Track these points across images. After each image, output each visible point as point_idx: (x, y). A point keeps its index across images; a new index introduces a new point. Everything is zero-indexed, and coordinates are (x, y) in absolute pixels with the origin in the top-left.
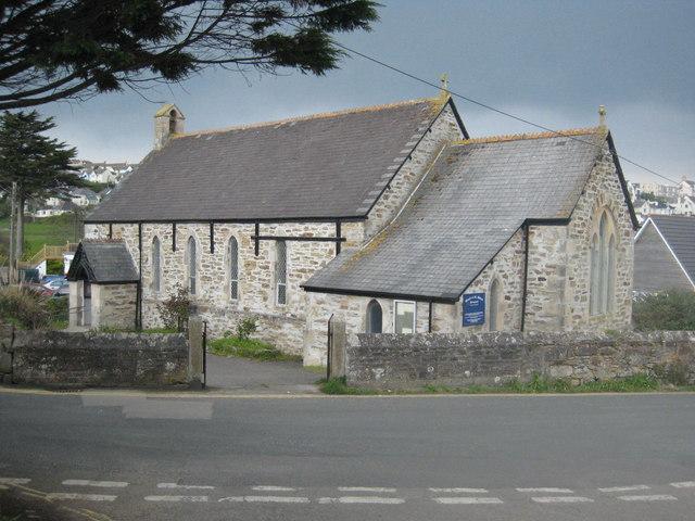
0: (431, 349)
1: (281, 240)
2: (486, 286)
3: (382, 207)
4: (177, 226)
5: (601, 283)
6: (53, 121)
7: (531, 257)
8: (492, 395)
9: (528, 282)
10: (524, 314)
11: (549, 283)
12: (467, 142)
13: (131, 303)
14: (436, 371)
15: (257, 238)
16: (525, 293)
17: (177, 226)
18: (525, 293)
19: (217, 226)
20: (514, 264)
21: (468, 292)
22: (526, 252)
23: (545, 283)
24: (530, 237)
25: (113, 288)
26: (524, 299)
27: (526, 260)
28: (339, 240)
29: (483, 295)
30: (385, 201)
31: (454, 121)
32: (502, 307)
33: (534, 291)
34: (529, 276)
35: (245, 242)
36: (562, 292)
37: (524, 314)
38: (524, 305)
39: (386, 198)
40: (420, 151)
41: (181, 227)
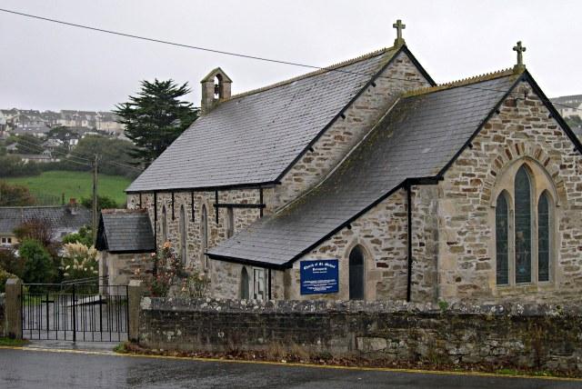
0: (220, 314)
1: (230, 207)
2: (342, 254)
3: (303, 171)
4: (175, 194)
5: (524, 246)
6: (186, 88)
7: (414, 220)
8: (272, 363)
9: (413, 248)
10: (409, 283)
11: (427, 249)
12: (434, 89)
13: (148, 272)
14: (226, 335)
15: (217, 206)
16: (410, 260)
17: (175, 194)
18: (410, 260)
19: (197, 195)
20: (392, 228)
21: (308, 258)
22: (410, 214)
23: (424, 248)
24: (412, 198)
25: (127, 257)
26: (410, 267)
27: (410, 223)
28: (262, 206)
29: (335, 262)
30: (306, 165)
31: (413, 69)
32: (373, 275)
33: (417, 257)
34: (413, 242)
35: (211, 210)
36: (436, 259)
37: (409, 283)
38: (410, 273)
39: (309, 160)
40: (358, 108)
41: (414, 188)
